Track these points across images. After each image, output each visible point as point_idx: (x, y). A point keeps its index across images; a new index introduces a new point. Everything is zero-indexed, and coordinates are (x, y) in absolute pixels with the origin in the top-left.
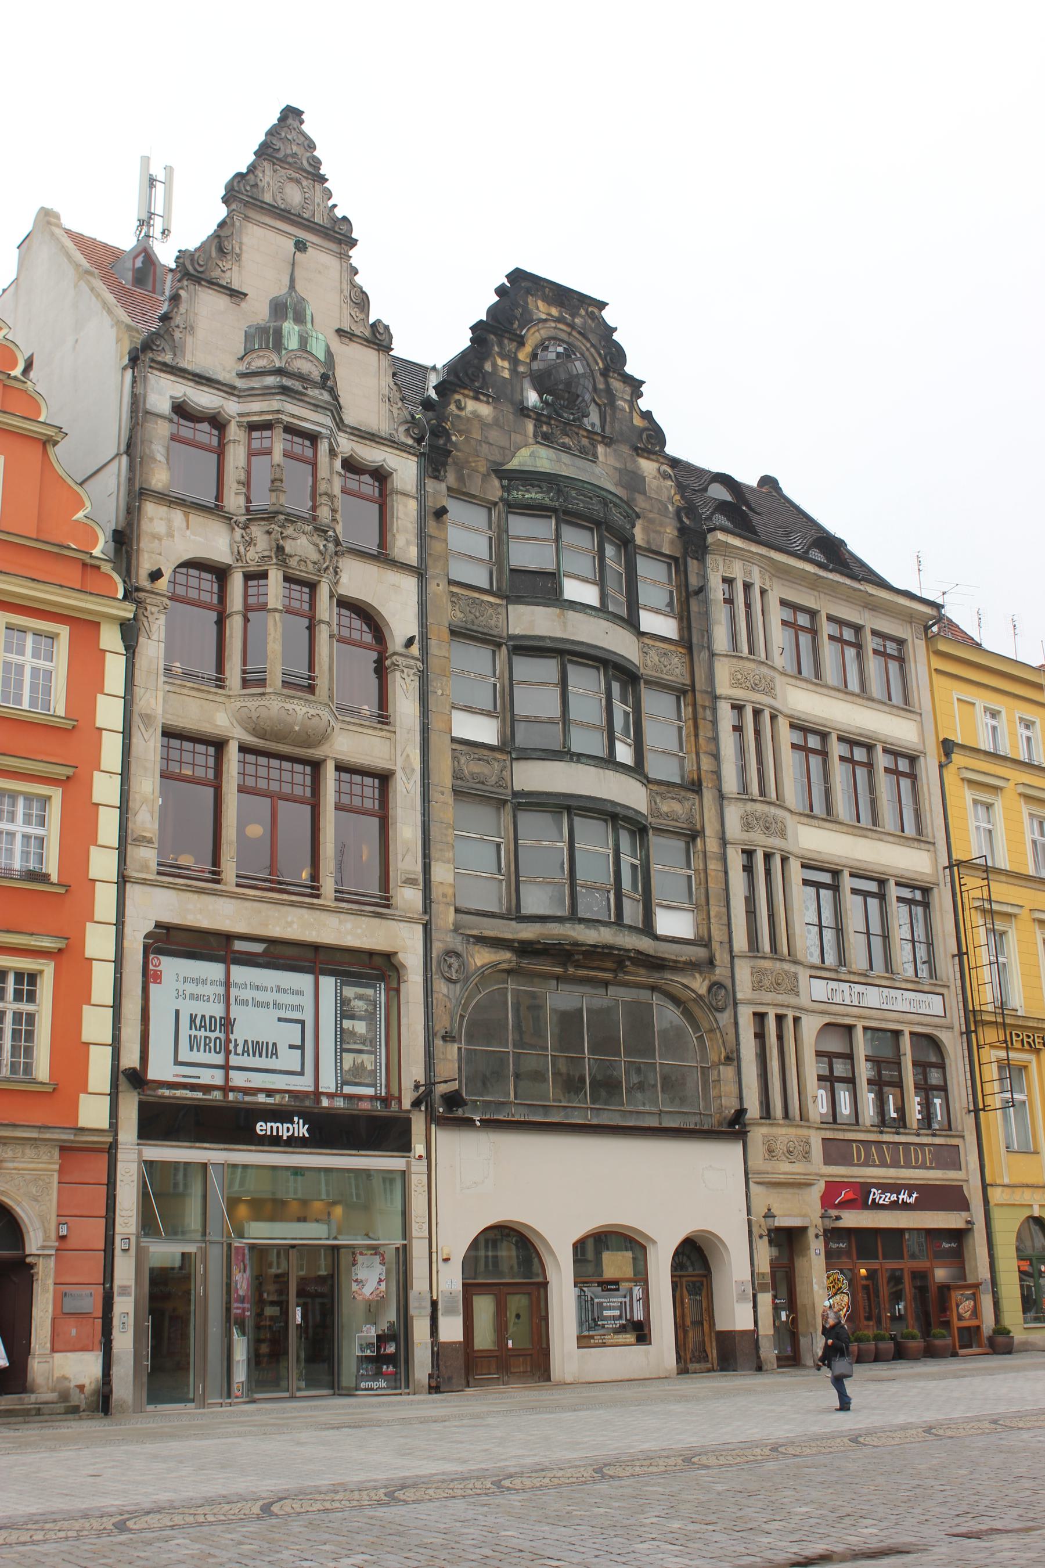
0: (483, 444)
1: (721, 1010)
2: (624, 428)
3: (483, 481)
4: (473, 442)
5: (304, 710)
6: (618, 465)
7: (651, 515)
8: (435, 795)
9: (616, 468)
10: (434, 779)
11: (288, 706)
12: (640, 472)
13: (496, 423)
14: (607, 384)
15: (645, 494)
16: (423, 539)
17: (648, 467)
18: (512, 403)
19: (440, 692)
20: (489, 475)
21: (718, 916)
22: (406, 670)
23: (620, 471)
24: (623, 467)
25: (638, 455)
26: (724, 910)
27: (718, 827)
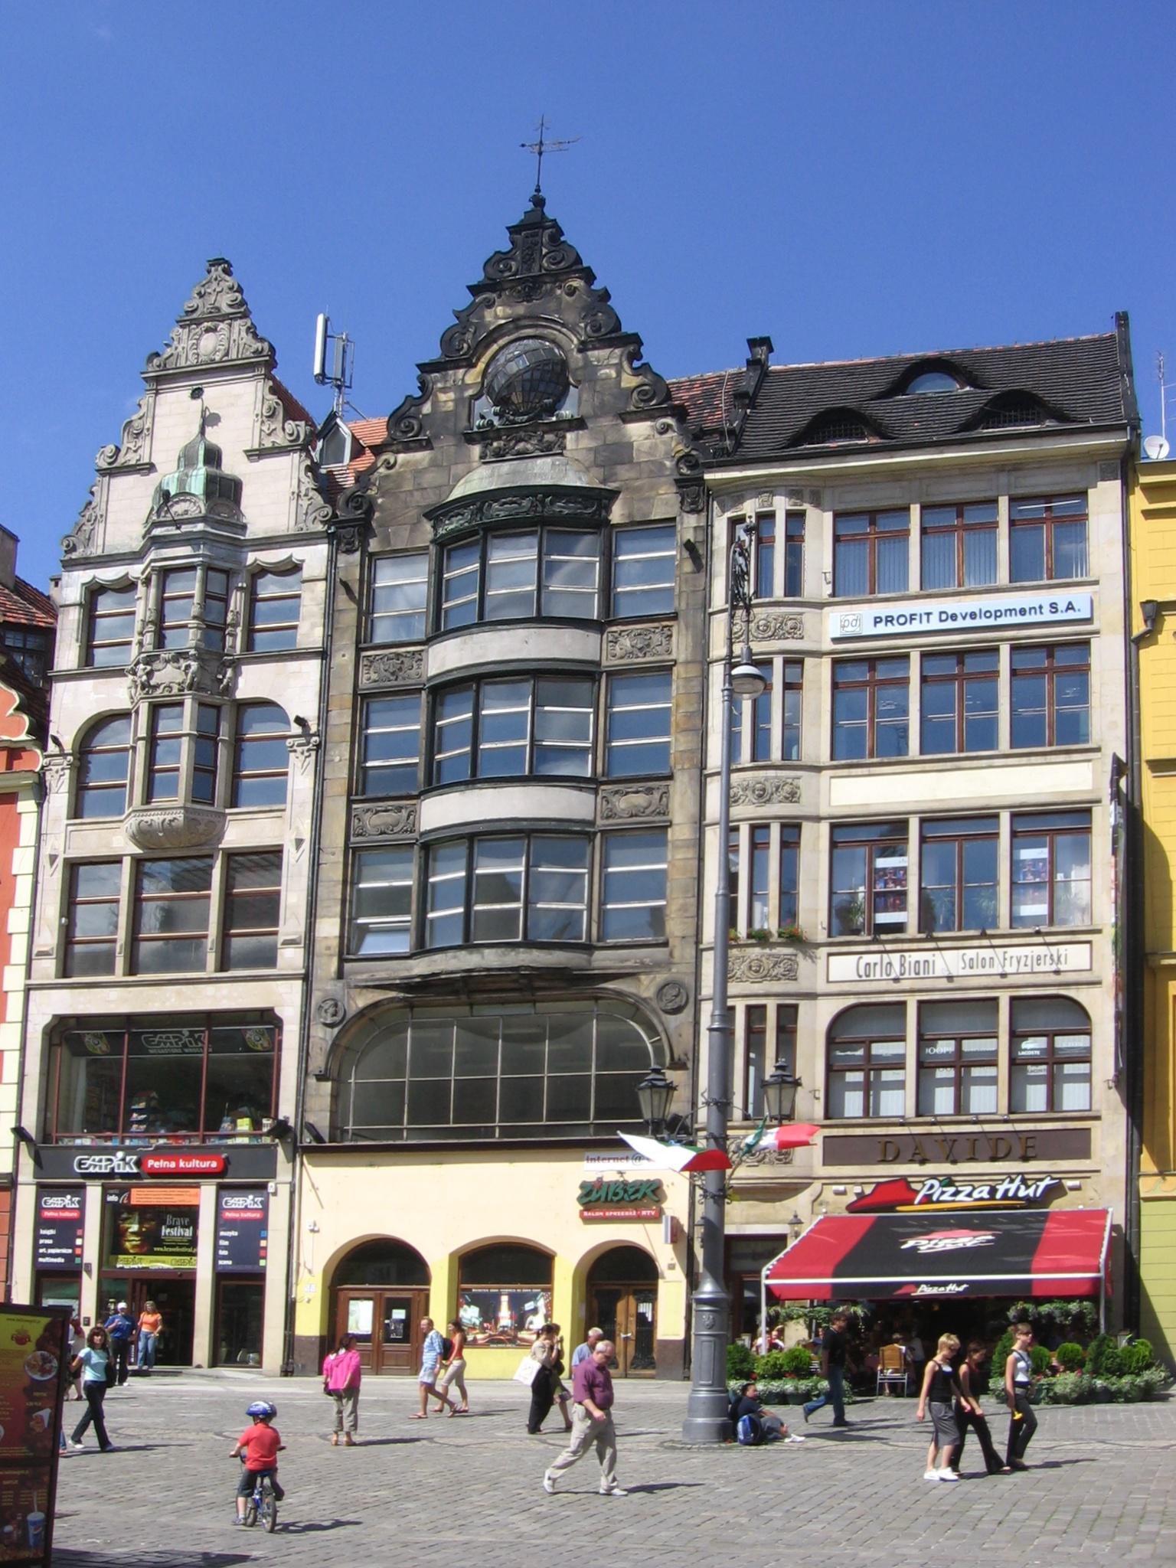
0: (416, 493)
1: (677, 1011)
2: (606, 398)
3: (412, 531)
4: (403, 496)
5: (162, 818)
6: (593, 444)
7: (637, 483)
8: (324, 858)
9: (590, 449)
10: (325, 842)
11: (145, 819)
12: (625, 440)
13: (434, 464)
14: (586, 360)
15: (631, 461)
16: (330, 614)
17: (638, 431)
18: (454, 434)
19: (337, 759)
20: (419, 521)
21: (684, 908)
22: (299, 749)
23: (595, 451)
24: (600, 443)
25: (625, 422)
26: (694, 901)
27: (695, 810)
